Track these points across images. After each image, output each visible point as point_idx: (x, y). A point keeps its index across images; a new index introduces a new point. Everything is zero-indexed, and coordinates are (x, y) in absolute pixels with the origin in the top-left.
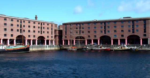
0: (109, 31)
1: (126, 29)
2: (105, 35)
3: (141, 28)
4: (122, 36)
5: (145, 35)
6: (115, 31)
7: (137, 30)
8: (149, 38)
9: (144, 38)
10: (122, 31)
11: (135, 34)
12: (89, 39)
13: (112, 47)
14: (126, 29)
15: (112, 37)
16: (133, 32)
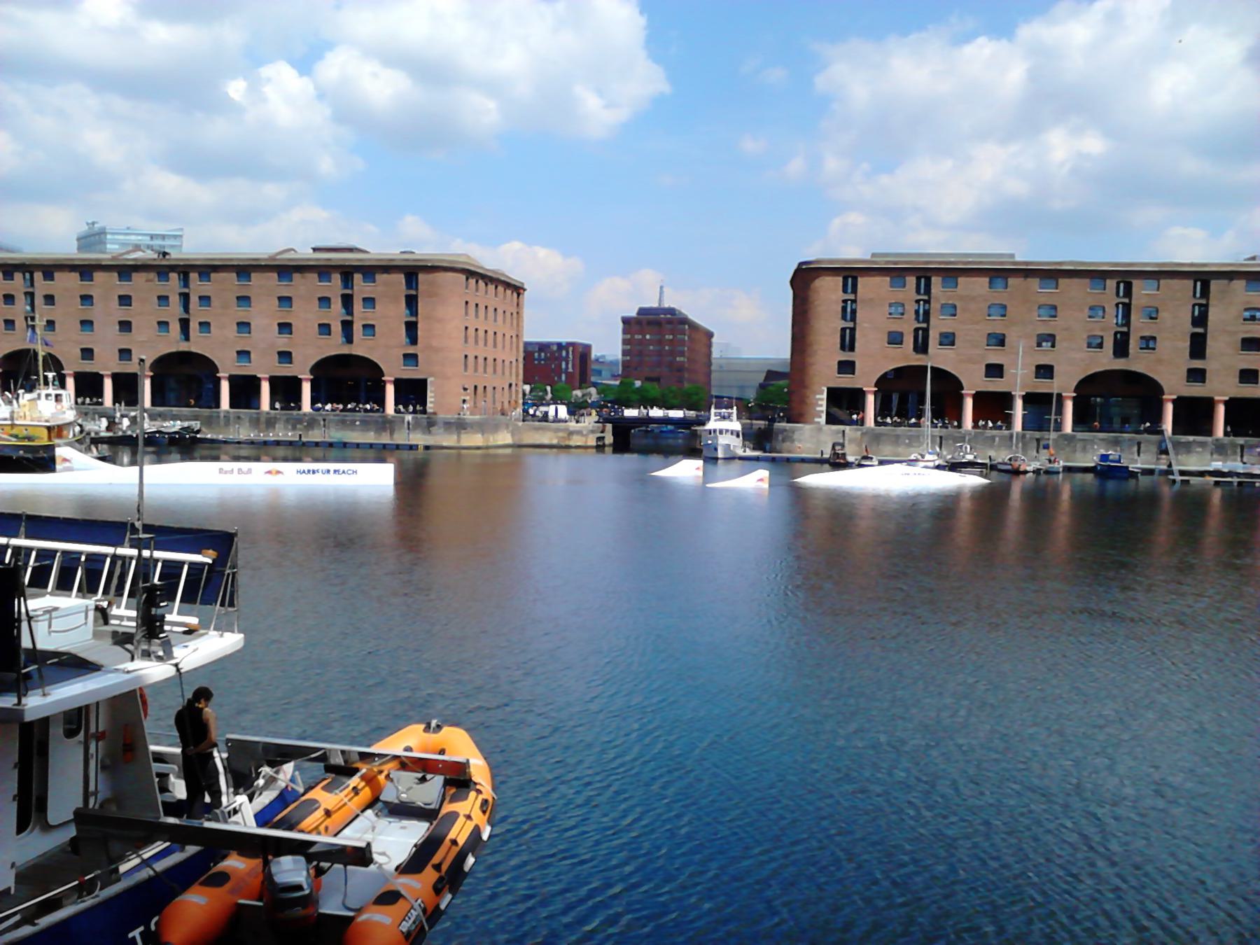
0: (205, 325)
2: (184, 347)
3: (391, 314)
5: (411, 358)
6: (244, 326)
7: (369, 328)
8: (432, 375)
9: (410, 373)
10: (285, 327)
11: (361, 347)
12: (88, 367)
13: (222, 423)
14: (306, 316)
15: (227, 366)
16: (349, 339)
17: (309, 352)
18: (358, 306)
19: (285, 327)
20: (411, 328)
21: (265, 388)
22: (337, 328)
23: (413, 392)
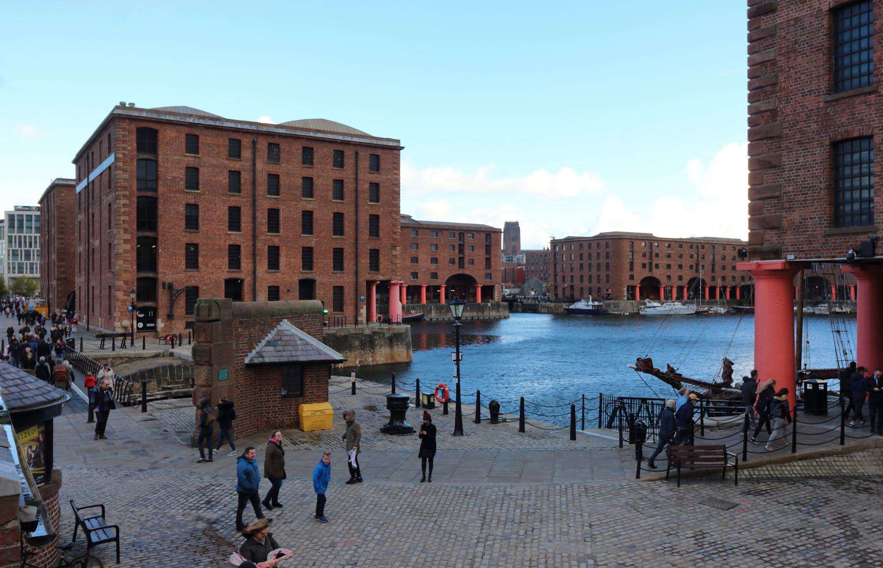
1: (445, 255)
4: (435, 275)
5: (489, 276)
7: (472, 262)
9: (488, 282)
16: (461, 265)
17: (446, 272)
18: (468, 251)
19: (435, 260)
20: (488, 260)
21: (424, 290)
22: (457, 261)
23: (488, 292)
